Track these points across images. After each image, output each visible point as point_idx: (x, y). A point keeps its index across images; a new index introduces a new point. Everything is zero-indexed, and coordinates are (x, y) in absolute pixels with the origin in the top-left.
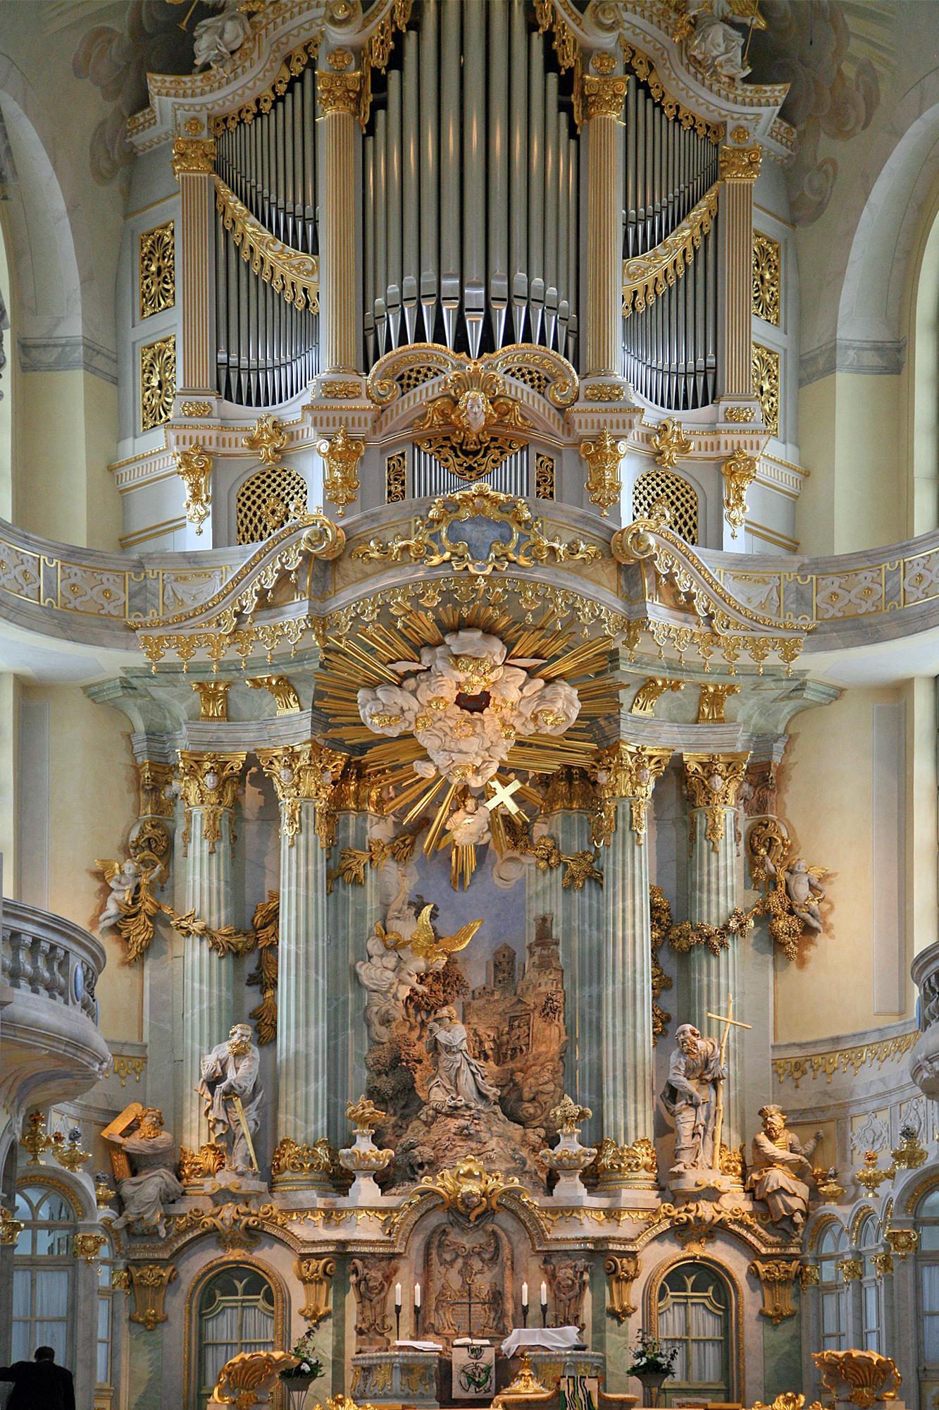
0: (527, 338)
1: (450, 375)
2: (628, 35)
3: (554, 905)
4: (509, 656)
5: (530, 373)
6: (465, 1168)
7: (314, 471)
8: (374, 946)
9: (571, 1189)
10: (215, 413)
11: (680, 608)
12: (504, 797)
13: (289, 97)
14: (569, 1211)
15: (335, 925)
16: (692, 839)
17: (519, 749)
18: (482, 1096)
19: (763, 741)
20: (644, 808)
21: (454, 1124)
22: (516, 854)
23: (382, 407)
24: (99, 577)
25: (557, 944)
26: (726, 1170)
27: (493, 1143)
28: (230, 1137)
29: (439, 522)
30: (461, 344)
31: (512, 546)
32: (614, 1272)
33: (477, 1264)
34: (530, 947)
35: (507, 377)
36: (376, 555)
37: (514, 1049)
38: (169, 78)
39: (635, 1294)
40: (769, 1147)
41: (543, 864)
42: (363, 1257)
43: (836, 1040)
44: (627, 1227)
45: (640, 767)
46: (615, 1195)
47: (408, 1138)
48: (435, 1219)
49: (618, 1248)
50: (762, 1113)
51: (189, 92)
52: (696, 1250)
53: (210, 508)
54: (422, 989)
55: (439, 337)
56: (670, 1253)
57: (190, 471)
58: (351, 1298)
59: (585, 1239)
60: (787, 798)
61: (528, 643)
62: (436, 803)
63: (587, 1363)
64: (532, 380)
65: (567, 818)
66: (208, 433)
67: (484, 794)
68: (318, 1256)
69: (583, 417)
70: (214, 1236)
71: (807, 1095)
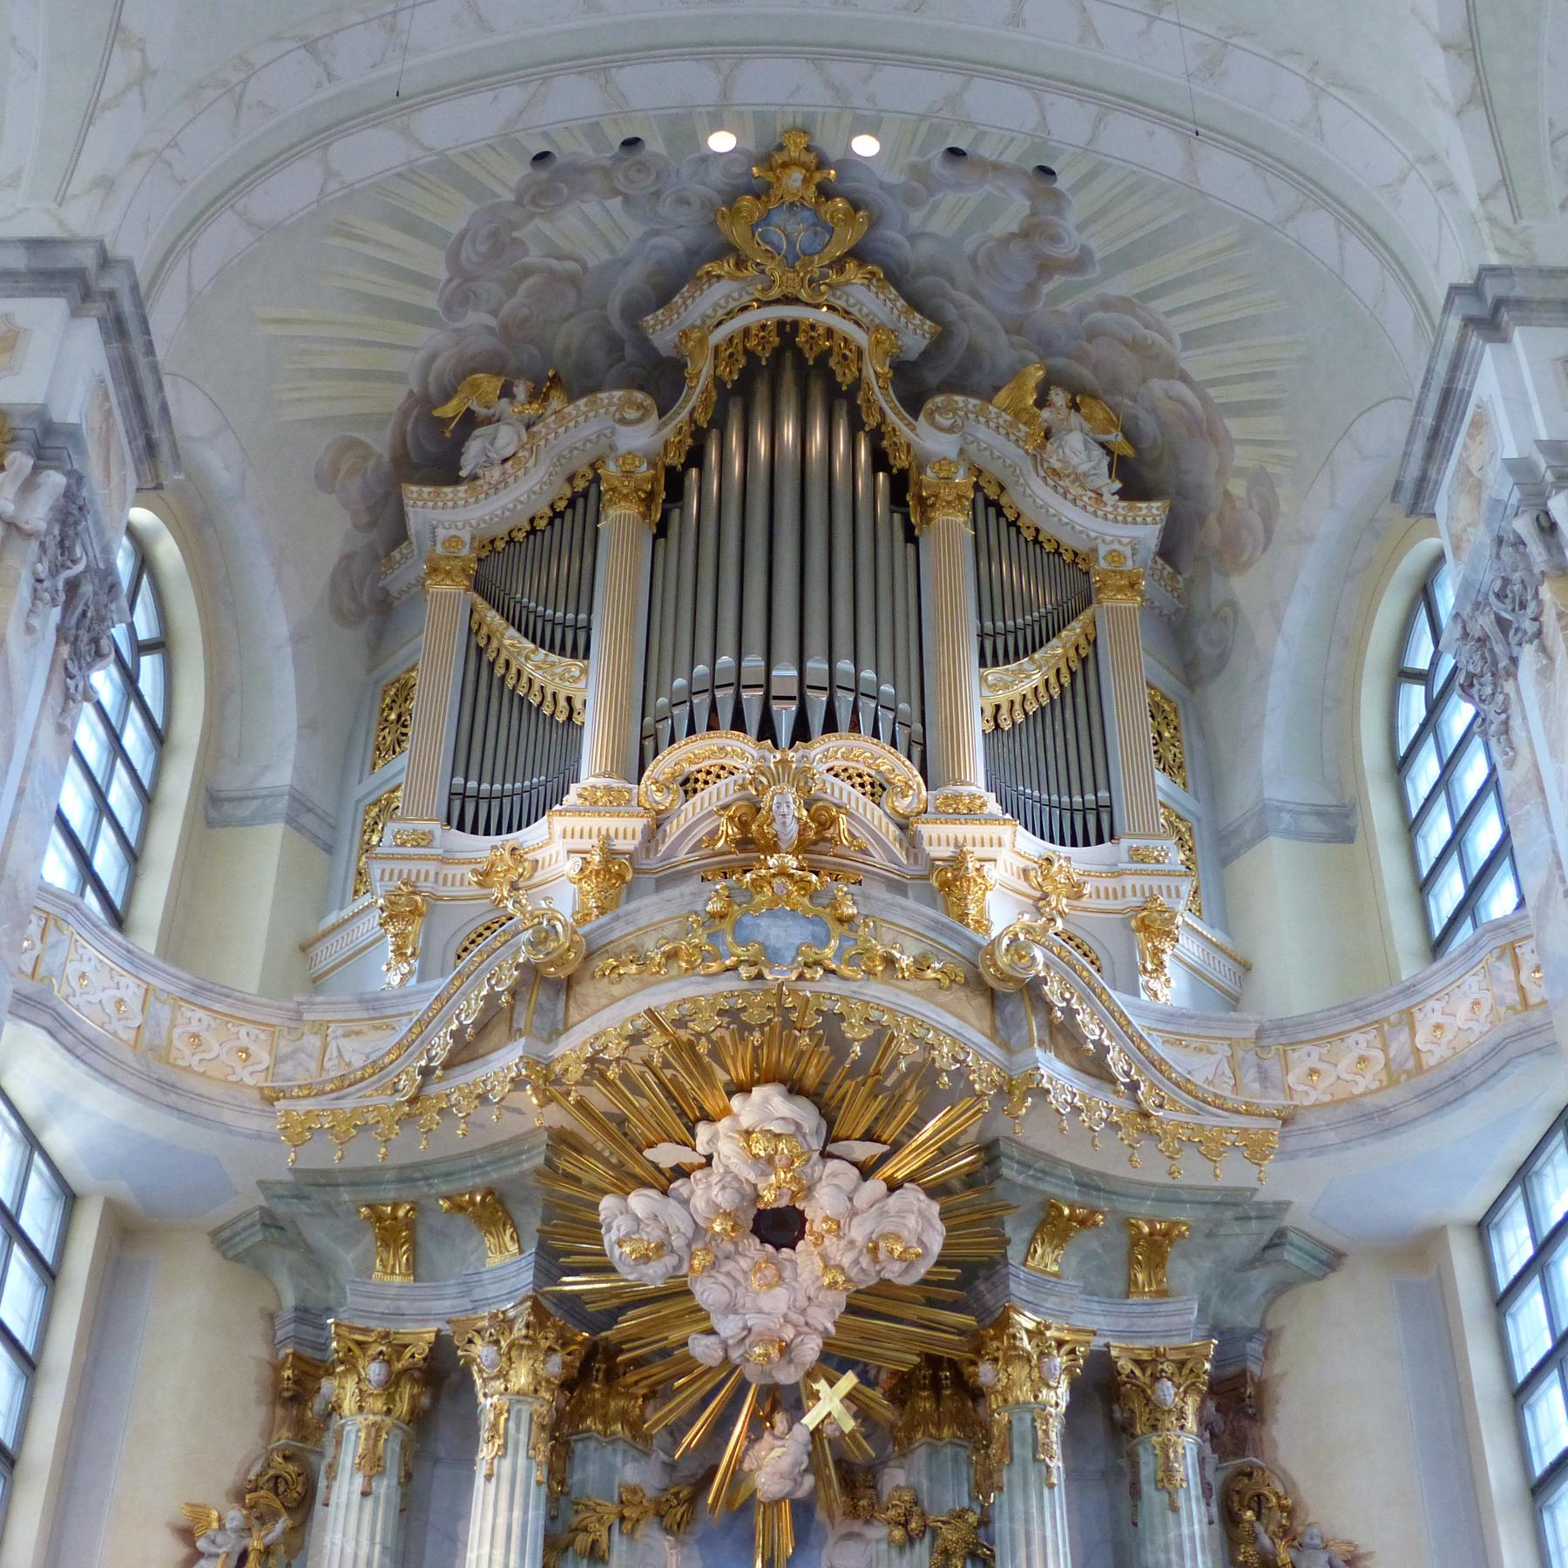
5: (860, 775)
10: (436, 843)
12: (830, 1403)
13: (569, 513)
17: (853, 1320)
22: (857, 1526)
23: (658, 822)
24: (234, 1030)
30: (767, 731)
31: (829, 952)
35: (830, 777)
38: (426, 490)
41: (898, 1533)
51: (450, 504)
53: (415, 963)
64: (862, 785)
65: (934, 1452)
66: (423, 866)
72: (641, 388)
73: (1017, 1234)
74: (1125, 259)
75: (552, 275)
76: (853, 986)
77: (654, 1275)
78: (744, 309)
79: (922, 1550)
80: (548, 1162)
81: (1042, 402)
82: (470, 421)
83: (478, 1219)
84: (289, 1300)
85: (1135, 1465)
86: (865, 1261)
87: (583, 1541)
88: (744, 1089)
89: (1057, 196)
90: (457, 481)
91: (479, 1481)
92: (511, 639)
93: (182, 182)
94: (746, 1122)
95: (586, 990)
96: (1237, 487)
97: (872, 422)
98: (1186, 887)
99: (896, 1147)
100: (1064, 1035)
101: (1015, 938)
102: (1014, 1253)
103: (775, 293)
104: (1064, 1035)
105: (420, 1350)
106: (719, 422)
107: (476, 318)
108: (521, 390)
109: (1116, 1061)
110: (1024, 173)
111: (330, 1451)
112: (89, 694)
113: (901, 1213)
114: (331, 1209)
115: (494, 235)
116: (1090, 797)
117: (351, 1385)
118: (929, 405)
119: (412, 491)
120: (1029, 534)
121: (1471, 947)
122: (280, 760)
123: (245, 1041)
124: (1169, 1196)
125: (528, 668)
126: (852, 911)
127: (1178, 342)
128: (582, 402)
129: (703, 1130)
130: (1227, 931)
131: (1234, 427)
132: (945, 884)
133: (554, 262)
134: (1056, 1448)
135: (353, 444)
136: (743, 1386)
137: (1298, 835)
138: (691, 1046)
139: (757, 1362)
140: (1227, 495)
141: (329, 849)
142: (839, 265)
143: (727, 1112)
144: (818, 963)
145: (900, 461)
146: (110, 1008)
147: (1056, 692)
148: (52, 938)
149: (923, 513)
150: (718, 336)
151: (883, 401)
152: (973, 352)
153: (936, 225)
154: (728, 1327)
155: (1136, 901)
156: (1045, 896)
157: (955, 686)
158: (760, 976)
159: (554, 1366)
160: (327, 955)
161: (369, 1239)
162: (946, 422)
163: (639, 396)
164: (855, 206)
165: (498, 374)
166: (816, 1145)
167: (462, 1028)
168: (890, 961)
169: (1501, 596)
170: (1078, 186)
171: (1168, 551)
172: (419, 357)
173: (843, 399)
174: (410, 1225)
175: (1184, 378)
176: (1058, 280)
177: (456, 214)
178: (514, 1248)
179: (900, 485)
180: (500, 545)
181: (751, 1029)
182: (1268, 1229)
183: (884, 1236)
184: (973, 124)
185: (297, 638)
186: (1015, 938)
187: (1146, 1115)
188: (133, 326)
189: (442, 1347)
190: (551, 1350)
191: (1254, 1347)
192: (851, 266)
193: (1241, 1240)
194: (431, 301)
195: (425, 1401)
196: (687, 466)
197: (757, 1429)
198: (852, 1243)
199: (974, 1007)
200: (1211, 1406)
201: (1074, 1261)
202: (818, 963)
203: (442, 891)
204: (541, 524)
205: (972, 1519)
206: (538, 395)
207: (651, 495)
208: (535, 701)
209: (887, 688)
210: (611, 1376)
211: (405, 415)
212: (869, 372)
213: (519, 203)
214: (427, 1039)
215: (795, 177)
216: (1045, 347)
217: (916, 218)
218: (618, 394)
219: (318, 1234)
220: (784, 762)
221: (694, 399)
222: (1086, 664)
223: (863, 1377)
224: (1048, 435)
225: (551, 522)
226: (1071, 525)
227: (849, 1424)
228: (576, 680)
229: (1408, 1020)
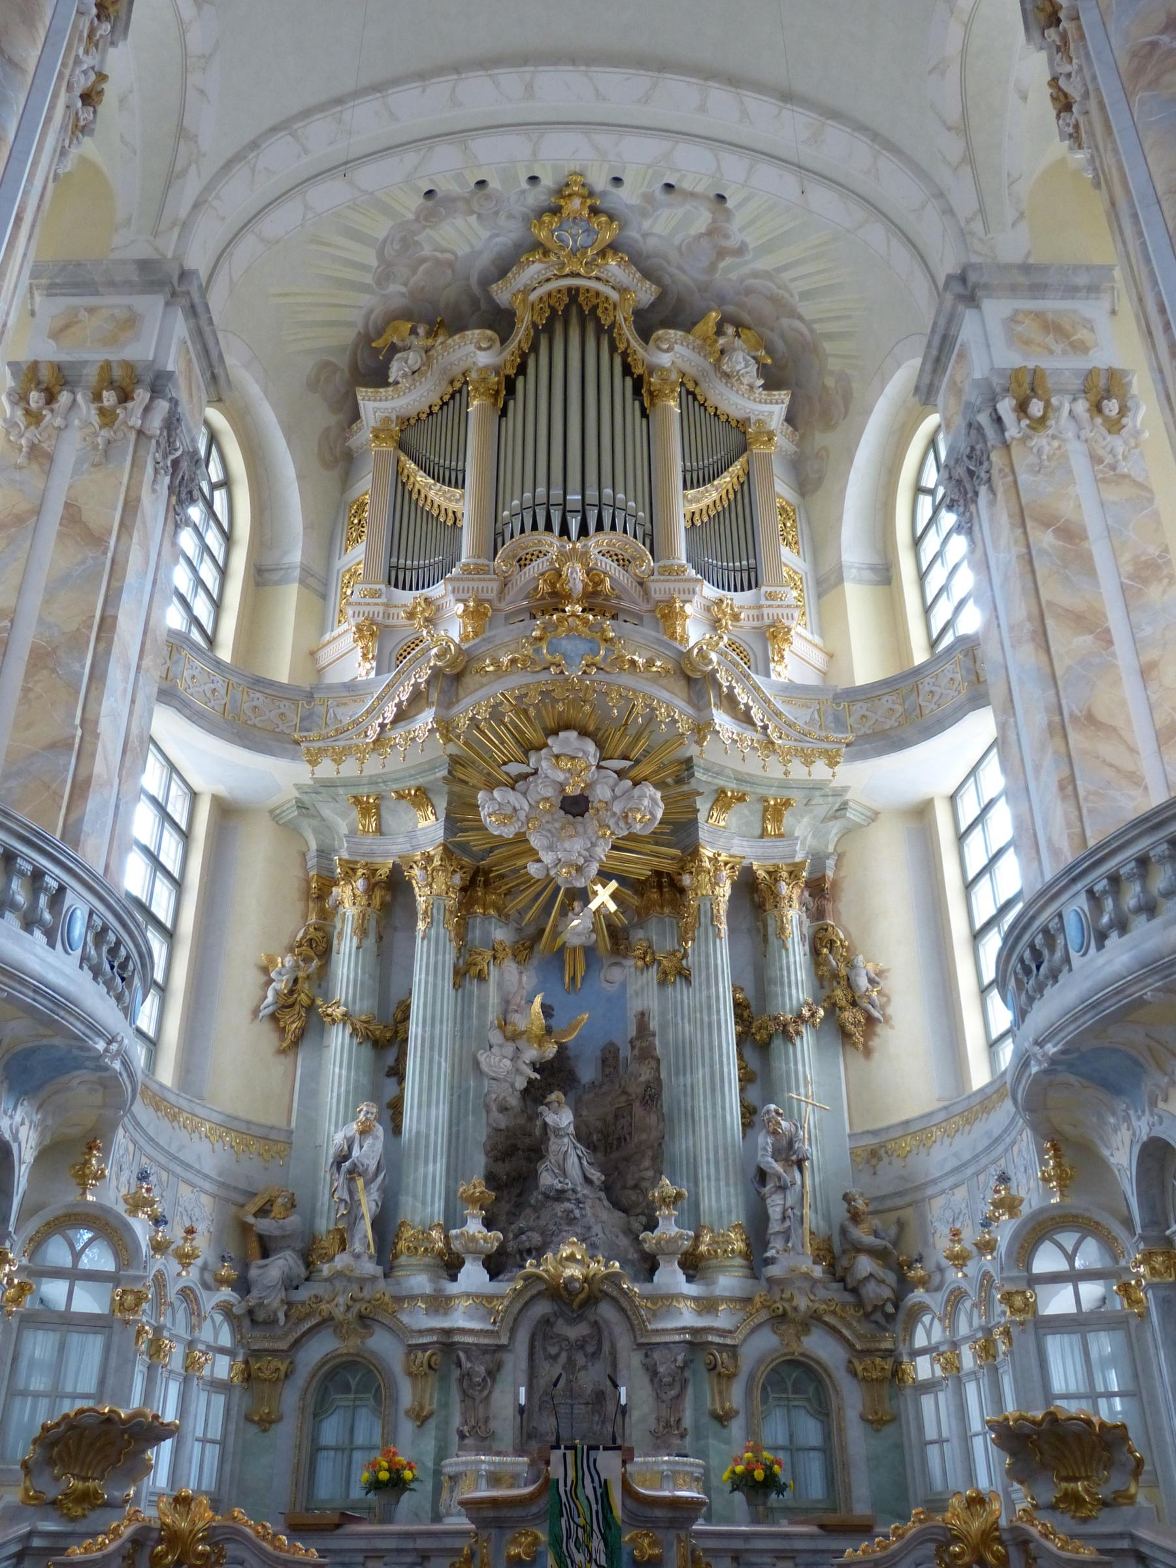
0: (613, 528)
1: (554, 551)
4: (602, 759)
12: (603, 897)
14: (667, 1300)
22: (618, 959)
25: (654, 1035)
29: (540, 639)
30: (565, 531)
32: (715, 1368)
34: (631, 1042)
36: (491, 668)
37: (619, 1139)
39: (736, 1395)
41: (640, 963)
46: (709, 1282)
49: (717, 1340)
55: (549, 528)
57: (361, 638)
59: (684, 1330)
63: (687, 1473)
67: (585, 896)
69: (657, 586)
72: (490, 327)
73: (703, 805)
74: (766, 249)
75: (438, 262)
76: (613, 677)
77: (509, 832)
78: (548, 280)
79: (654, 970)
80: (450, 772)
81: (720, 332)
82: (393, 349)
83: (414, 804)
84: (313, 846)
85: (765, 926)
86: (622, 824)
87: (474, 971)
88: (555, 732)
89: (727, 211)
90: (387, 385)
91: (419, 941)
92: (421, 479)
93: (223, 219)
94: (556, 750)
95: (469, 680)
96: (830, 382)
97: (622, 347)
98: (797, 614)
99: (637, 762)
100: (730, 702)
101: (701, 649)
102: (701, 817)
103: (567, 270)
104: (730, 702)
105: (384, 872)
106: (535, 348)
107: (395, 288)
108: (421, 330)
109: (757, 715)
110: (708, 198)
111: (339, 925)
112: (188, 522)
113: (641, 797)
115: (404, 239)
116: (744, 563)
117: (348, 890)
118: (654, 336)
119: (362, 393)
120: (712, 411)
121: (950, 649)
123: (283, 710)
124: (785, 785)
125: (432, 494)
126: (612, 634)
127: (797, 298)
128: (457, 337)
130: (822, 636)
131: (828, 346)
132: (664, 616)
133: (438, 254)
134: (724, 919)
135: (326, 365)
136: (558, 888)
137: (860, 581)
138: (525, 712)
139: (563, 875)
140: (824, 386)
141: (324, 597)
142: (602, 253)
143: (546, 745)
144: (594, 664)
145: (638, 370)
146: (209, 694)
147: (726, 504)
148: (175, 656)
149: (652, 400)
150: (533, 297)
151: (628, 333)
152: (680, 301)
153: (657, 229)
154: (548, 858)
155: (767, 621)
156: (719, 620)
158: (562, 672)
159: (457, 880)
160: (326, 656)
161: (355, 813)
162: (665, 346)
163: (489, 332)
164: (611, 218)
165: (409, 320)
166: (594, 763)
167: (401, 702)
168: (633, 663)
169: (970, 457)
170: (740, 205)
171: (790, 419)
172: (363, 312)
173: (606, 332)
174: (378, 807)
175: (800, 318)
176: (728, 261)
177: (381, 228)
178: (433, 818)
179: (638, 384)
180: (413, 421)
181: (557, 701)
182: (839, 801)
183: (631, 810)
184: (679, 171)
185: (300, 477)
186: (701, 649)
187: (773, 743)
188: (200, 309)
189: (396, 870)
190: (454, 871)
191: (831, 863)
192: (610, 253)
193: (822, 807)
194: (368, 279)
195: (388, 898)
196: (516, 375)
197: (565, 910)
198: (614, 814)
200: (806, 894)
201: (734, 820)
202: (594, 664)
203: (390, 622)
204: (435, 409)
205: (679, 955)
206: (432, 333)
207: (497, 392)
208: (435, 513)
209: (631, 504)
210: (487, 884)
211: (356, 346)
212: (620, 317)
213: (417, 220)
214: (382, 708)
215: (576, 203)
216: (721, 300)
217: (646, 224)
218: (477, 331)
219: (327, 811)
220: (574, 549)
221: (521, 334)
222: (745, 486)
223: (622, 880)
224: (722, 352)
225: (441, 408)
226: (736, 404)
227: (612, 907)
228: (457, 501)
229: (916, 689)
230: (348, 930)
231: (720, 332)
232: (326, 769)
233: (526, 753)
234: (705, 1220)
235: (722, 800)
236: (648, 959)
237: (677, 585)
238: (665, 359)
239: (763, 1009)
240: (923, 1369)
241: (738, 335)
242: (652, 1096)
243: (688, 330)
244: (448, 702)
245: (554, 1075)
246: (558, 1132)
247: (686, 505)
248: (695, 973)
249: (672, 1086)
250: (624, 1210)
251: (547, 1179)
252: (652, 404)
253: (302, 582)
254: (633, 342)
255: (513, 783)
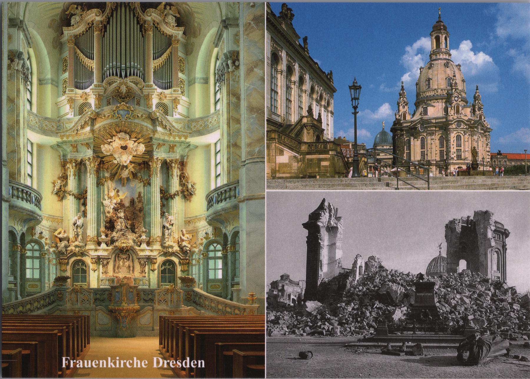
2: (153, 18)
3: (142, 190)
6: (123, 241)
7: (92, 101)
8: (106, 197)
9: (144, 246)
11: (164, 128)
12: (131, 167)
15: (99, 193)
16: (168, 176)
18: (127, 228)
19: (182, 157)
20: (159, 170)
21: (121, 233)
26: (174, 242)
27: (129, 237)
28: (78, 235)
30: (121, 76)
33: (125, 260)
40: (183, 238)
42: (103, 259)
43: (196, 216)
44: (155, 253)
45: (158, 161)
46: (152, 247)
47: (113, 235)
48: (117, 252)
50: (182, 231)
52: (169, 258)
54: (115, 206)
55: (117, 75)
56: (163, 258)
58: (101, 266)
60: (187, 168)
61: (134, 135)
62: (118, 169)
65: (144, 172)
68: (94, 258)
70: (75, 255)
71: (190, 228)
73: (155, 147)
77: (108, 154)
81: (165, 8)
106: (112, 15)
114: (66, 145)
122: (49, 76)
129: (114, 137)
151: (139, 10)
154: (118, 159)
157: (148, 64)
159: (97, 164)
189: (82, 161)
199: (149, 121)
209: (139, 66)
219: (64, 147)
221: (108, 10)
222: (170, 58)
227: (133, 170)
230: (72, 174)
231: (165, 8)
232: (65, 139)
233: (112, 137)
234: (152, 235)
235: (159, 145)
236: (141, 180)
237: (150, 90)
238: (149, 18)
239: (167, 191)
240: (194, 262)
241: (170, 9)
242: (141, 210)
243: (156, 8)
244: (93, 125)
245: (120, 205)
246: (121, 218)
247: (153, 64)
248: (152, 184)
249: (146, 208)
250: (135, 233)
251: (119, 227)
252: (145, 33)
253: (52, 84)
254: (140, 13)
255: (109, 143)
